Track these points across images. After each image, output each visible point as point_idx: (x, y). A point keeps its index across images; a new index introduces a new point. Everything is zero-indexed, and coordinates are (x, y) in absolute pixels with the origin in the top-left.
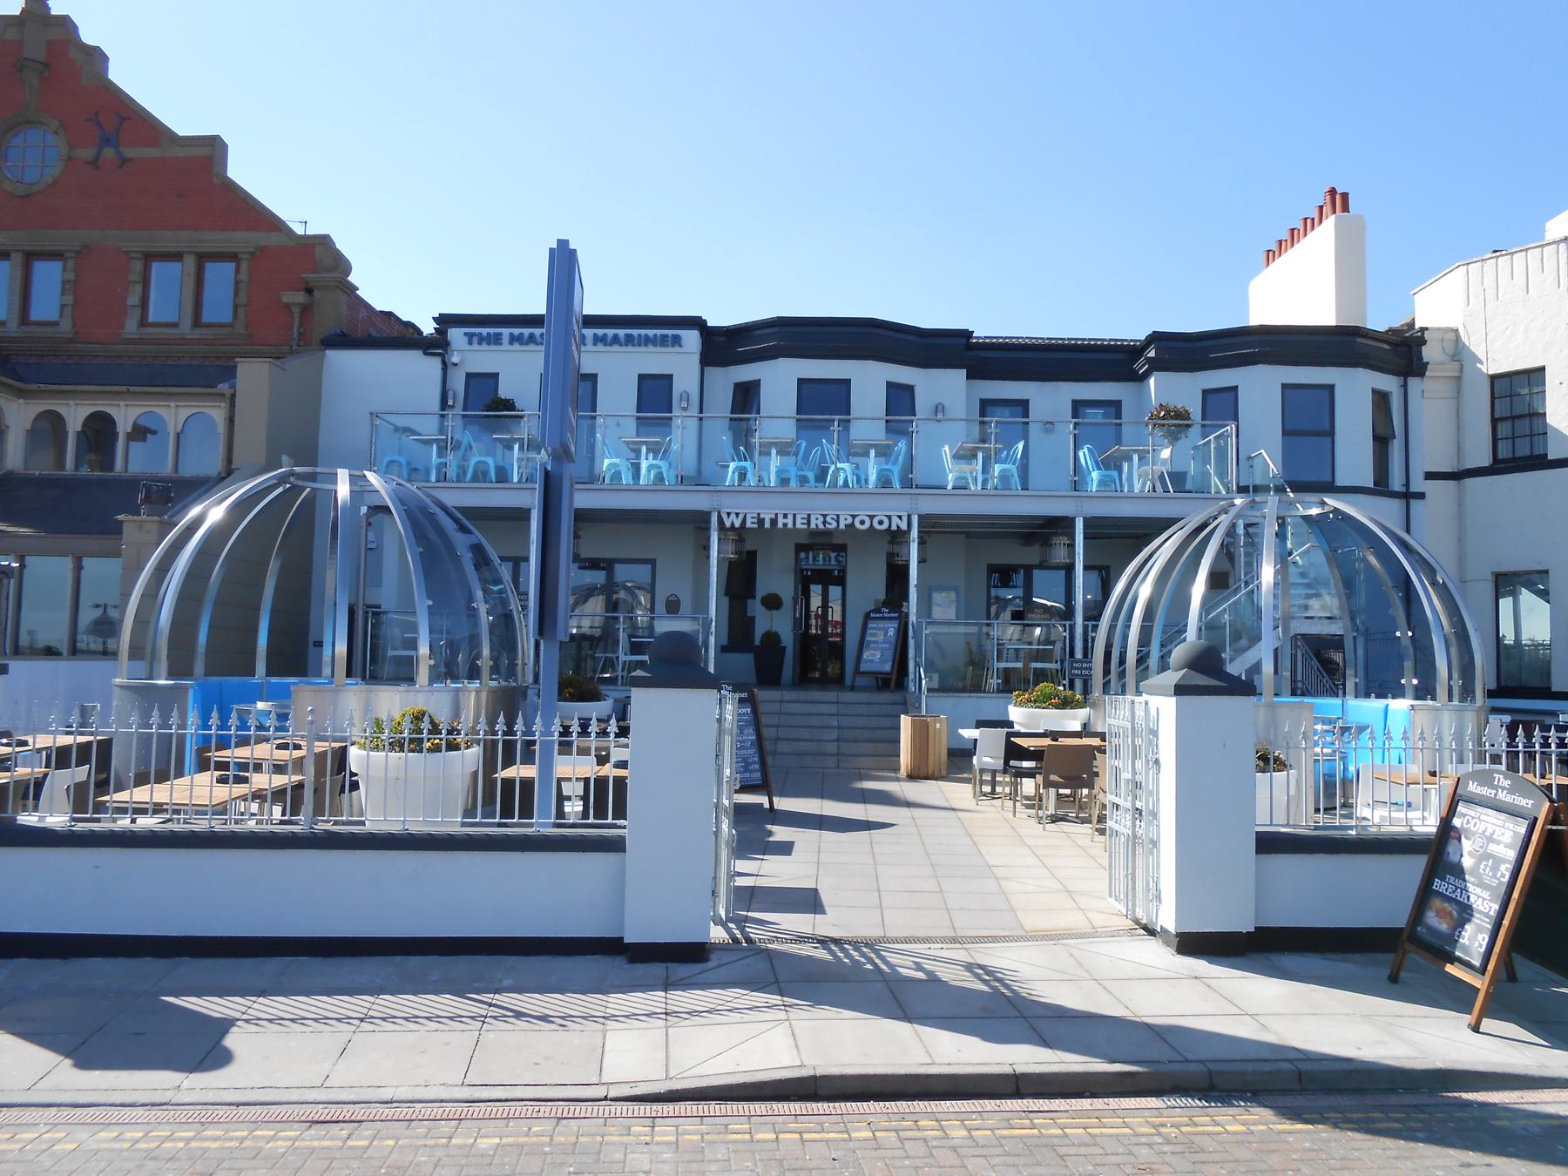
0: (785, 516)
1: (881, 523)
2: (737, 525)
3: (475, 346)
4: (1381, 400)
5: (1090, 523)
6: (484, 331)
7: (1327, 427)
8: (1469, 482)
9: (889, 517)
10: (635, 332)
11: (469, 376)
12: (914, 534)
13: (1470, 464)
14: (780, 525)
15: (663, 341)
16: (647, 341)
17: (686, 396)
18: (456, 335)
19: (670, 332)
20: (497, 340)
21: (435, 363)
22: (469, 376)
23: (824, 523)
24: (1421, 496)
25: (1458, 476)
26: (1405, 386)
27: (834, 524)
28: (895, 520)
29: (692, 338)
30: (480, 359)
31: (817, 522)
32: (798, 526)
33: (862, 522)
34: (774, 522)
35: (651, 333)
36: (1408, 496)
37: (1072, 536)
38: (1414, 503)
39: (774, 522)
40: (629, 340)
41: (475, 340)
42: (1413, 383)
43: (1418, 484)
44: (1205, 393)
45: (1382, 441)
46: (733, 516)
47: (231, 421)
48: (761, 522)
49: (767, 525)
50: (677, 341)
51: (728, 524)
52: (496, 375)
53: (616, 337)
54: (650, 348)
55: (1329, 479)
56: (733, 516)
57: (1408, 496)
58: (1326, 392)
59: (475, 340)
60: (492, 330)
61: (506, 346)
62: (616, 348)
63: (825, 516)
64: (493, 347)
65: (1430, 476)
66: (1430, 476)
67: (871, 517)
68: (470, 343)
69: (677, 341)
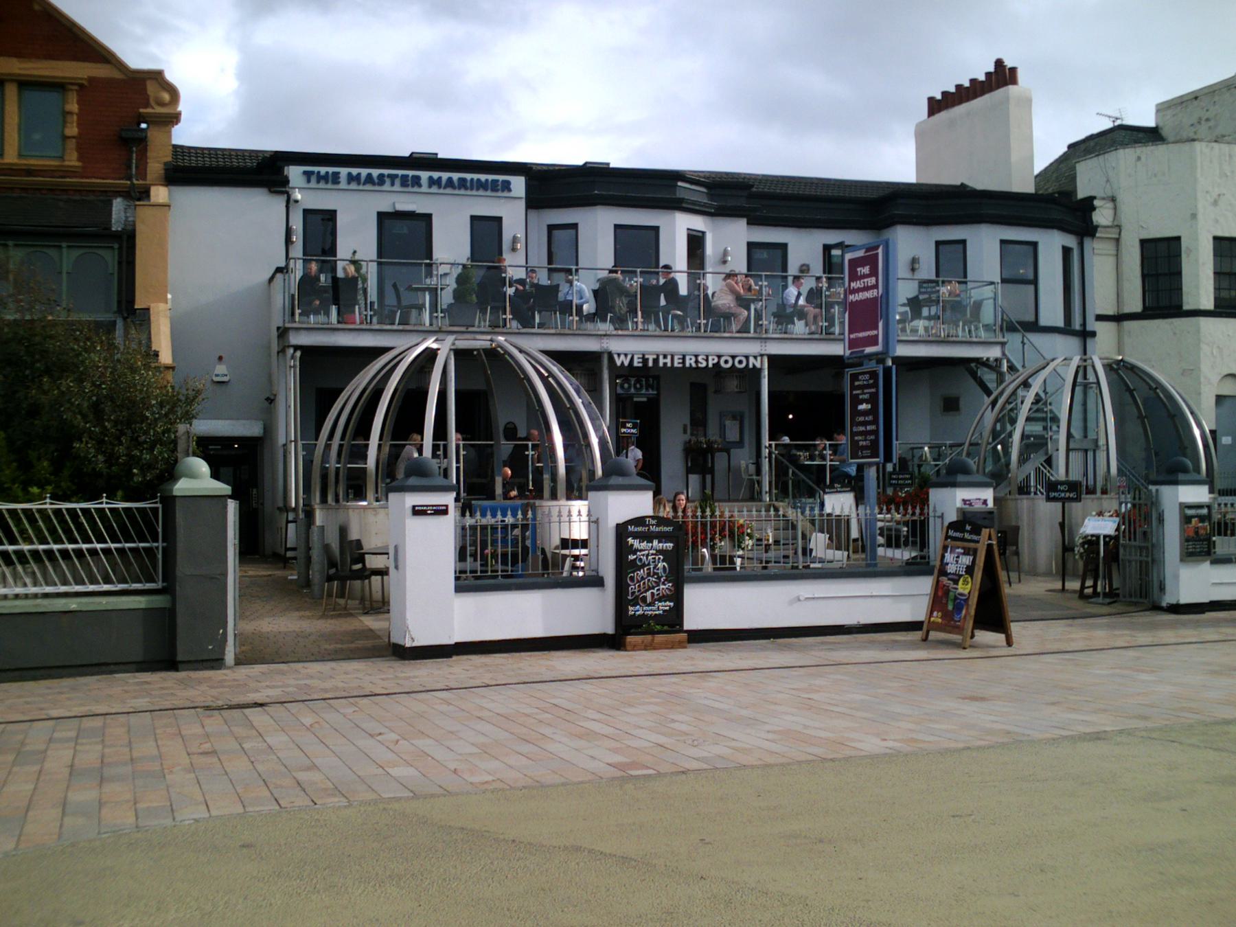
0: (665, 357)
2: (626, 363)
3: (313, 184)
4: (1067, 251)
6: (323, 170)
7: (1031, 276)
8: (1128, 325)
9: (747, 357)
10: (468, 176)
13: (1127, 309)
14: (661, 365)
15: (494, 186)
16: (482, 185)
18: (294, 173)
23: (697, 362)
24: (1093, 334)
25: (1119, 318)
27: (704, 364)
28: (752, 360)
29: (518, 184)
31: (690, 362)
32: (676, 365)
34: (656, 361)
35: (483, 177)
39: (656, 361)
40: (463, 183)
41: (314, 179)
43: (1092, 325)
46: (622, 357)
48: (645, 361)
49: (651, 364)
50: (507, 186)
51: (619, 363)
53: (450, 179)
55: (1031, 318)
56: (622, 357)
58: (1031, 248)
59: (314, 179)
60: (331, 170)
62: (449, 191)
63: (696, 356)
64: (330, 186)
65: (1100, 318)
66: (1100, 318)
68: (309, 181)
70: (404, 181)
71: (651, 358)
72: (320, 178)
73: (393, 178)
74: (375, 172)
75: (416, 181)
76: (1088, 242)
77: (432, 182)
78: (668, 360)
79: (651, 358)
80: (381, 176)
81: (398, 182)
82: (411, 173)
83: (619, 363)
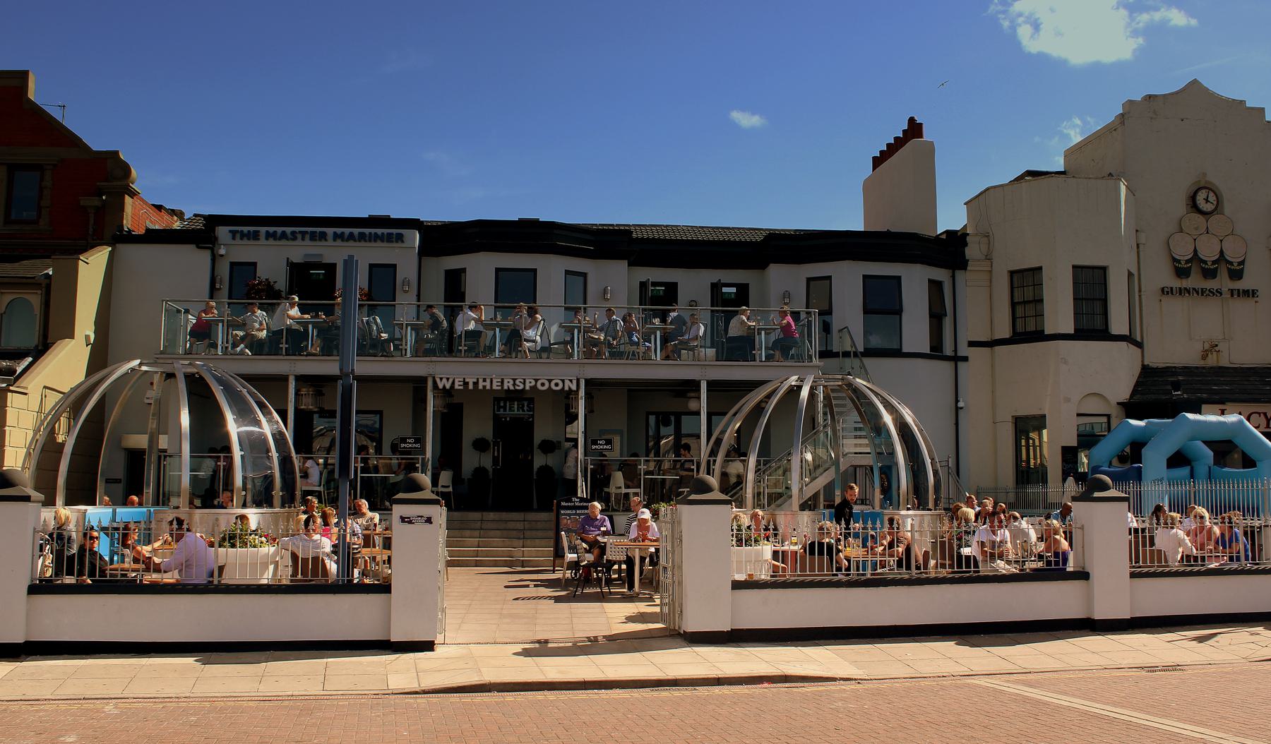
0: (484, 380)
1: (557, 385)
2: (448, 387)
3: (238, 241)
4: (935, 286)
5: (712, 385)
6: (245, 229)
9: (563, 381)
10: (367, 231)
11: (233, 264)
12: (582, 393)
13: (997, 337)
14: (481, 387)
15: (389, 238)
16: (376, 238)
17: (406, 282)
18: (222, 232)
19: (395, 231)
20: (256, 236)
21: (205, 256)
22: (233, 264)
23: (514, 384)
24: (965, 359)
26: (953, 277)
27: (521, 387)
28: (567, 383)
30: (244, 252)
31: (508, 385)
33: (543, 384)
34: (476, 384)
35: (379, 231)
36: (957, 359)
37: (699, 390)
38: (960, 364)
39: (476, 384)
40: (362, 237)
41: (238, 236)
42: (959, 274)
43: (964, 350)
44: (809, 280)
45: (936, 317)
47: (46, 305)
48: (466, 384)
49: (471, 387)
50: (400, 238)
51: (441, 386)
52: (254, 264)
53: (351, 234)
54: (379, 244)
55: (896, 346)
57: (957, 359)
59: (238, 236)
60: (252, 229)
61: (263, 241)
63: (514, 380)
65: (972, 344)
66: (972, 344)
67: (550, 381)
68: (234, 238)
69: (400, 238)
70: (313, 237)
71: (471, 381)
72: (243, 236)
73: (304, 233)
74: (289, 230)
75: (323, 236)
76: (959, 274)
77: (336, 236)
78: (488, 384)
79: (471, 381)
80: (293, 233)
81: (307, 237)
82: (318, 230)
83: (441, 386)
